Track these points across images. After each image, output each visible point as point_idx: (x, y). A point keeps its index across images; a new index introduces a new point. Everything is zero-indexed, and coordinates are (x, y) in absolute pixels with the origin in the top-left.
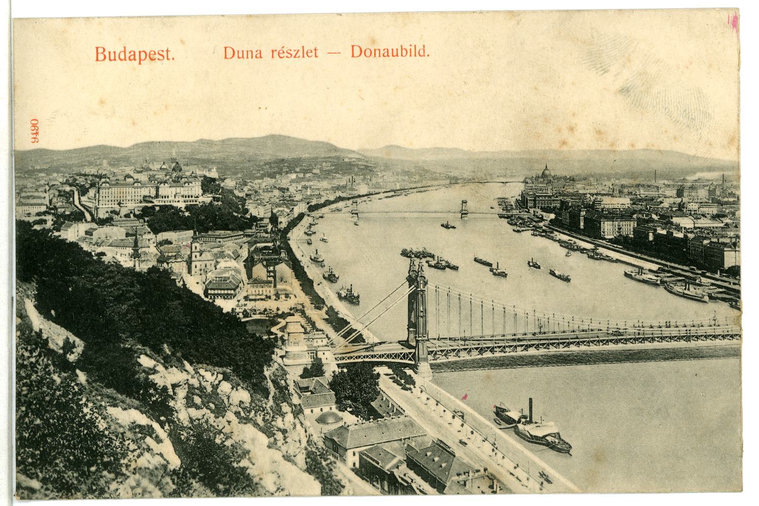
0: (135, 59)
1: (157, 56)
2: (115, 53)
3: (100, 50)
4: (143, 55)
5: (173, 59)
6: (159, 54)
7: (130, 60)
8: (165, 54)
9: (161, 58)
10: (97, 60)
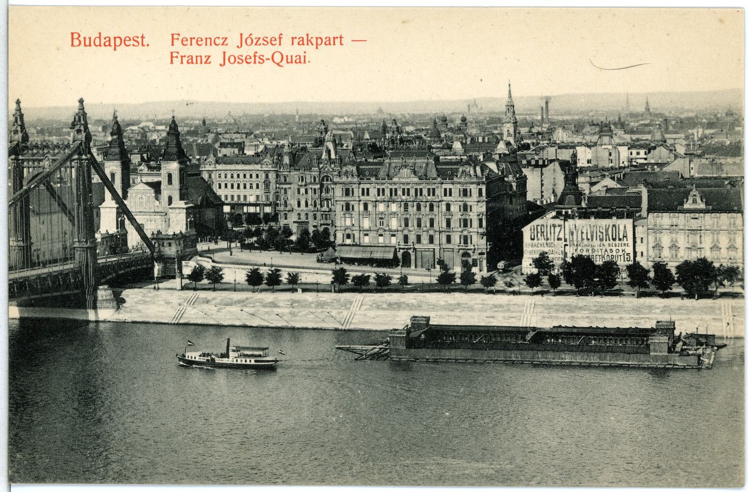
0: (110, 45)
1: (132, 42)
2: (90, 38)
3: (76, 36)
4: (118, 41)
5: (148, 45)
6: (134, 40)
7: (105, 45)
8: (140, 40)
9: (136, 44)
10: (73, 45)
